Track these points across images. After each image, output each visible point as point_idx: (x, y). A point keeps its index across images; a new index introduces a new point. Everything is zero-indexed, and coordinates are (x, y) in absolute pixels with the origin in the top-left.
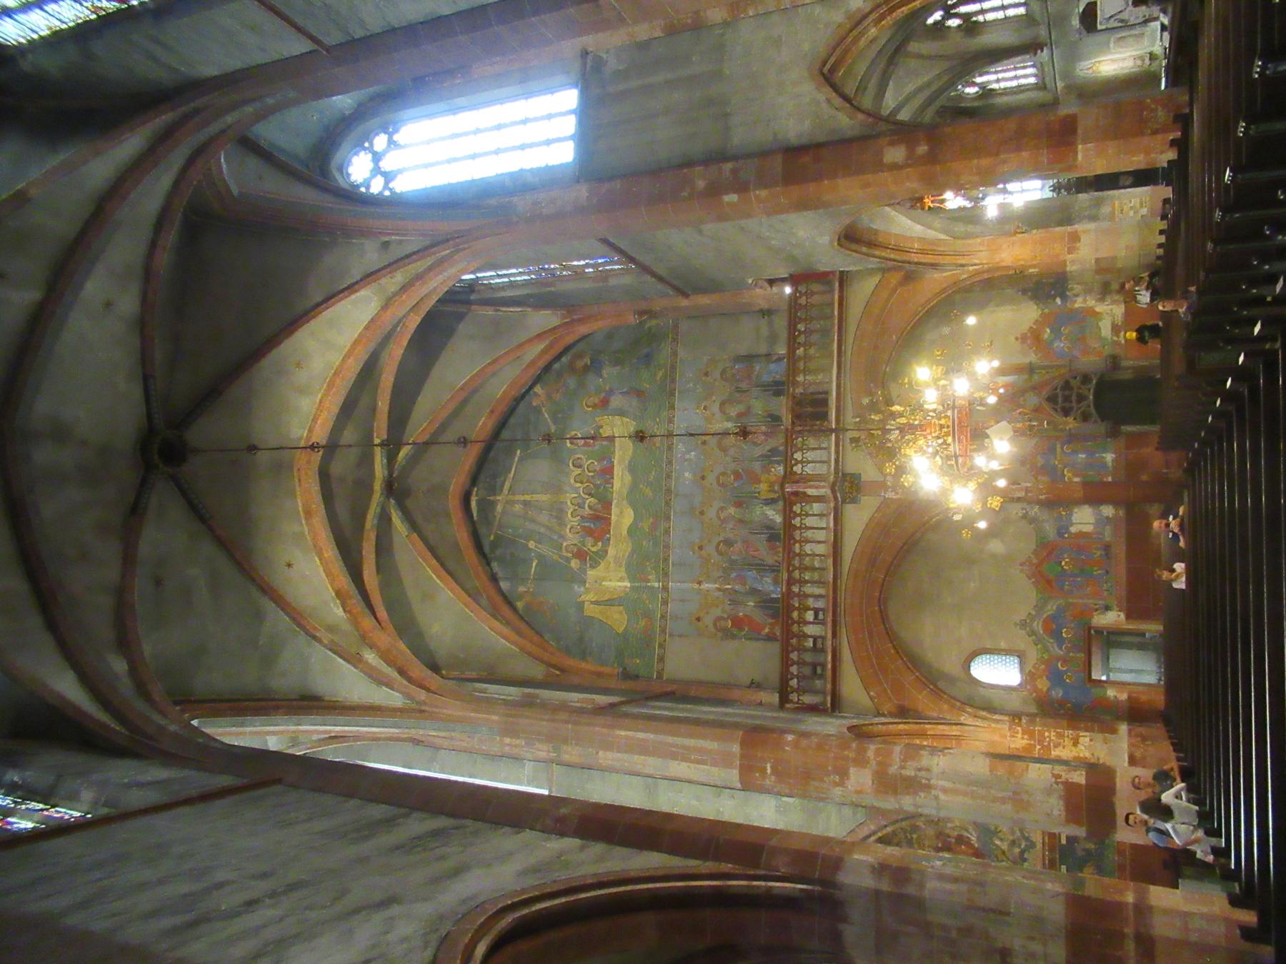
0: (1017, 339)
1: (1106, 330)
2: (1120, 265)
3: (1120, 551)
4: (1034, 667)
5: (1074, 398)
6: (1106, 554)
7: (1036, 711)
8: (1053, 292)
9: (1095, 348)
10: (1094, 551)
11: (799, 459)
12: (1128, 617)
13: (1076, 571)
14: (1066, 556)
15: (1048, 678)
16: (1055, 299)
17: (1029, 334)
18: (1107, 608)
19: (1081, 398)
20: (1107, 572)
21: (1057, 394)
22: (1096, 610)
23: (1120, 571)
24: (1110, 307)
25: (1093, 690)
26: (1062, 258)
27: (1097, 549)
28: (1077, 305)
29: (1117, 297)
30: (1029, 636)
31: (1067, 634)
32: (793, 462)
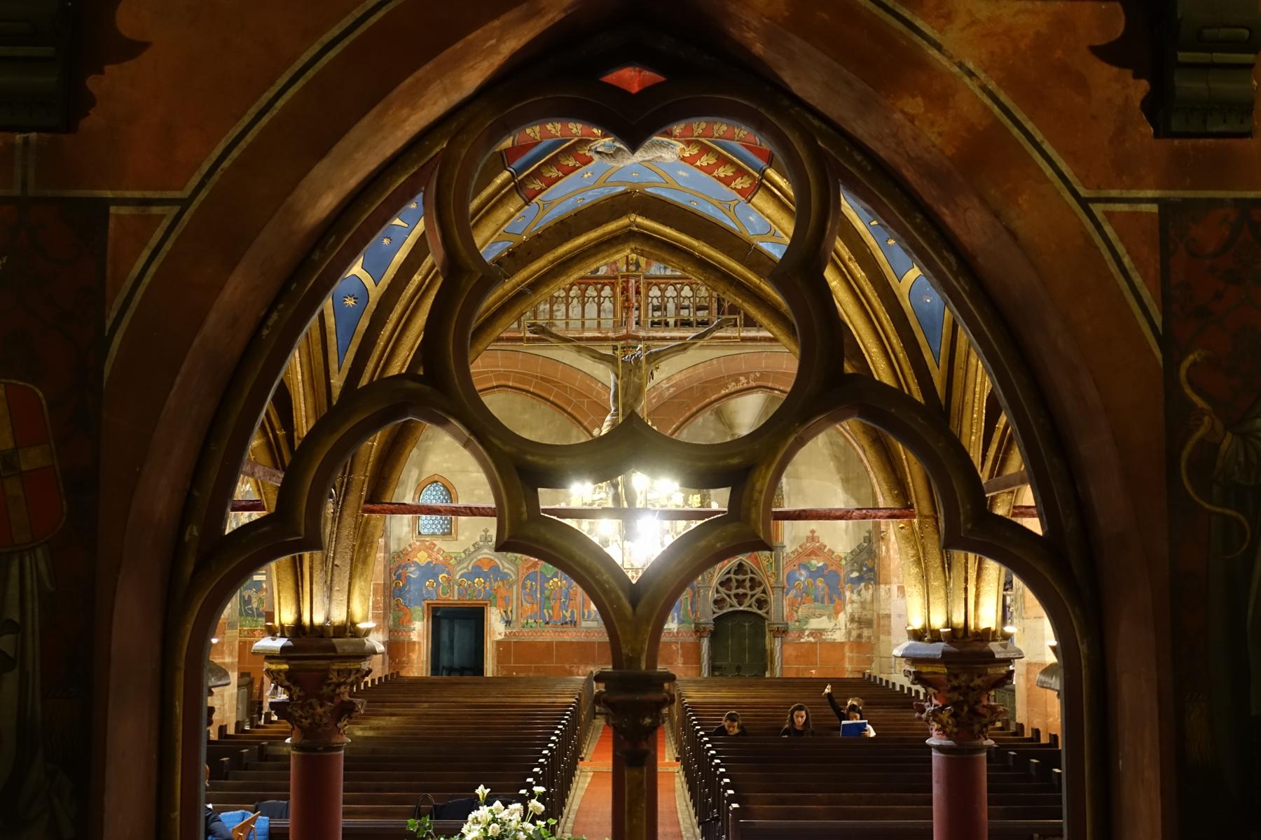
0: (813, 532)
1: (814, 624)
2: (882, 637)
3: (570, 636)
4: (440, 549)
5: (741, 591)
6: (566, 623)
7: (392, 551)
8: (865, 569)
9: (797, 612)
10: (570, 611)
11: (668, 294)
12: (499, 643)
13: (547, 593)
14: (564, 582)
15: (429, 563)
16: (857, 571)
17: (817, 544)
18: (508, 623)
19: (740, 598)
20: (547, 623)
21: (745, 573)
22: (505, 612)
23: (549, 635)
24: (843, 627)
25: (420, 609)
26: (895, 580)
27: (572, 613)
28: (848, 594)
29: (854, 633)
30: (474, 545)
31: (477, 583)
32: (663, 286)
